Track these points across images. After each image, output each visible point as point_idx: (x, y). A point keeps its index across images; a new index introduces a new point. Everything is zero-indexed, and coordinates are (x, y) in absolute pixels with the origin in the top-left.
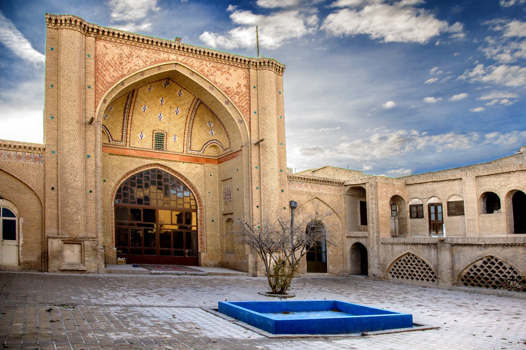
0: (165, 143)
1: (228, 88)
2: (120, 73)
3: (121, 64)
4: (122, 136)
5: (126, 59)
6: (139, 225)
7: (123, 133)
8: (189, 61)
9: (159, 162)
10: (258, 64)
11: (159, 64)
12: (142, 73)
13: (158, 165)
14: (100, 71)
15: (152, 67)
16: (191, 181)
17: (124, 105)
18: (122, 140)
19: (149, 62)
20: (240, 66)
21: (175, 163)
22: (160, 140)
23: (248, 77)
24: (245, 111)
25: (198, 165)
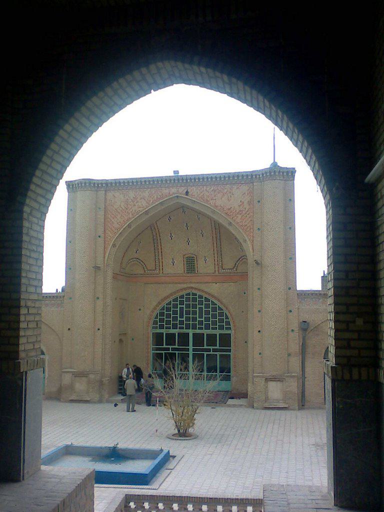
4: (156, 265)
10: (261, 176)
12: (147, 213)
13: (192, 288)
16: (224, 301)
19: (151, 201)
22: (191, 264)
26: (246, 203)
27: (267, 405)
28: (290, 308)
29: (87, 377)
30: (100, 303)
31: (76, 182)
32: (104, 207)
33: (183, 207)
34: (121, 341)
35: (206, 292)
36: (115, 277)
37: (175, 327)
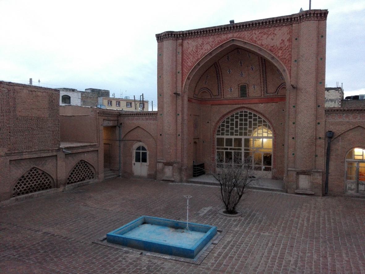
0: (247, 92)
1: (272, 47)
2: (196, 58)
3: (197, 52)
4: (219, 92)
5: (200, 47)
6: (231, 149)
7: (219, 90)
8: (242, 35)
9: (244, 105)
10: (299, 18)
11: (221, 44)
12: (210, 54)
13: (244, 107)
14: (185, 61)
15: (216, 47)
17: (216, 72)
18: (219, 95)
19: (214, 45)
20: (284, 25)
21: (255, 105)
22: (243, 90)
23: (290, 32)
24: (287, 61)
25: (273, 104)
26: (286, 40)
27: (296, 191)
28: (318, 121)
29: (172, 165)
30: (180, 118)
31: (163, 35)
32: (181, 51)
33: (238, 48)
34: (195, 143)
35: (254, 110)
36: (189, 100)
37: (232, 134)
